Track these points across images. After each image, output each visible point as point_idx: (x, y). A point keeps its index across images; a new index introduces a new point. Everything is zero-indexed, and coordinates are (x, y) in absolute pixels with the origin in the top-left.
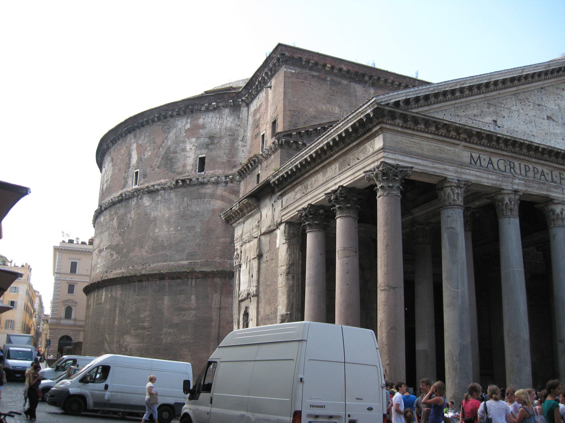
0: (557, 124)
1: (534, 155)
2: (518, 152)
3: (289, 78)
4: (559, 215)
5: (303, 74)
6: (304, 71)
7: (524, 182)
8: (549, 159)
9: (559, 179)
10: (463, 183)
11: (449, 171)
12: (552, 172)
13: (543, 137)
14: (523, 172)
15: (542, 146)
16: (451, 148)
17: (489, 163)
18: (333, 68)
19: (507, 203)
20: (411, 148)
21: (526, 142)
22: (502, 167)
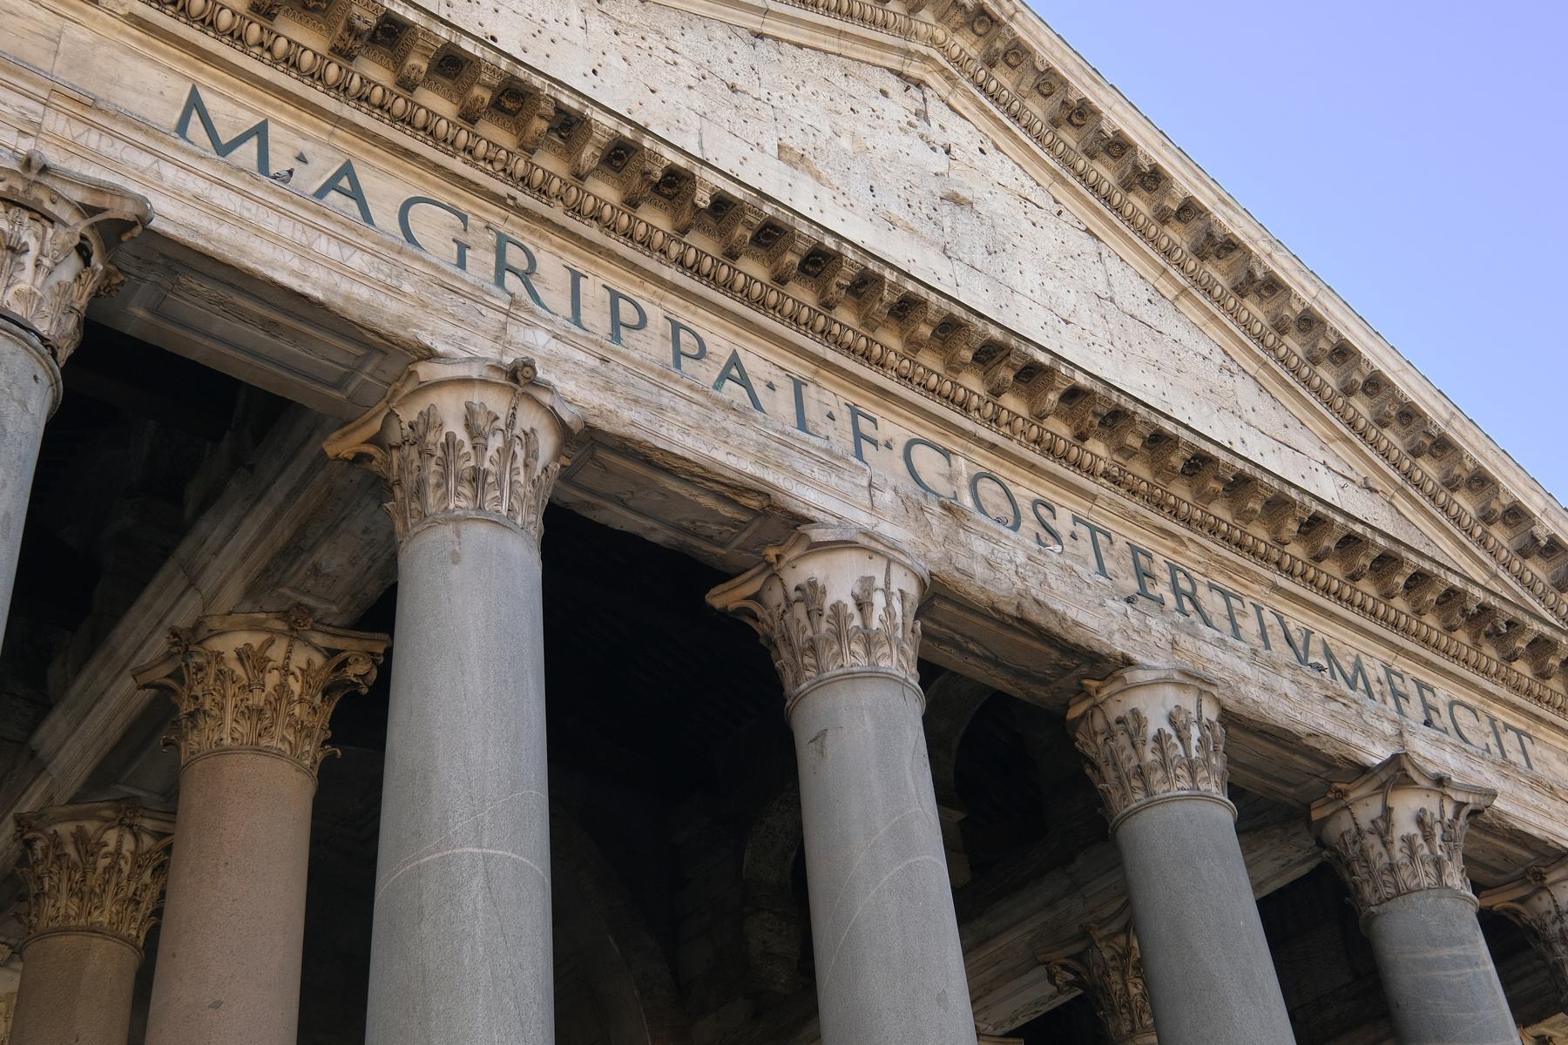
0: (843, 200)
2: (556, 183)
4: (852, 617)
8: (773, 298)
10: (78, 195)
12: (798, 385)
14: (596, 317)
17: (331, 185)
19: (450, 444)
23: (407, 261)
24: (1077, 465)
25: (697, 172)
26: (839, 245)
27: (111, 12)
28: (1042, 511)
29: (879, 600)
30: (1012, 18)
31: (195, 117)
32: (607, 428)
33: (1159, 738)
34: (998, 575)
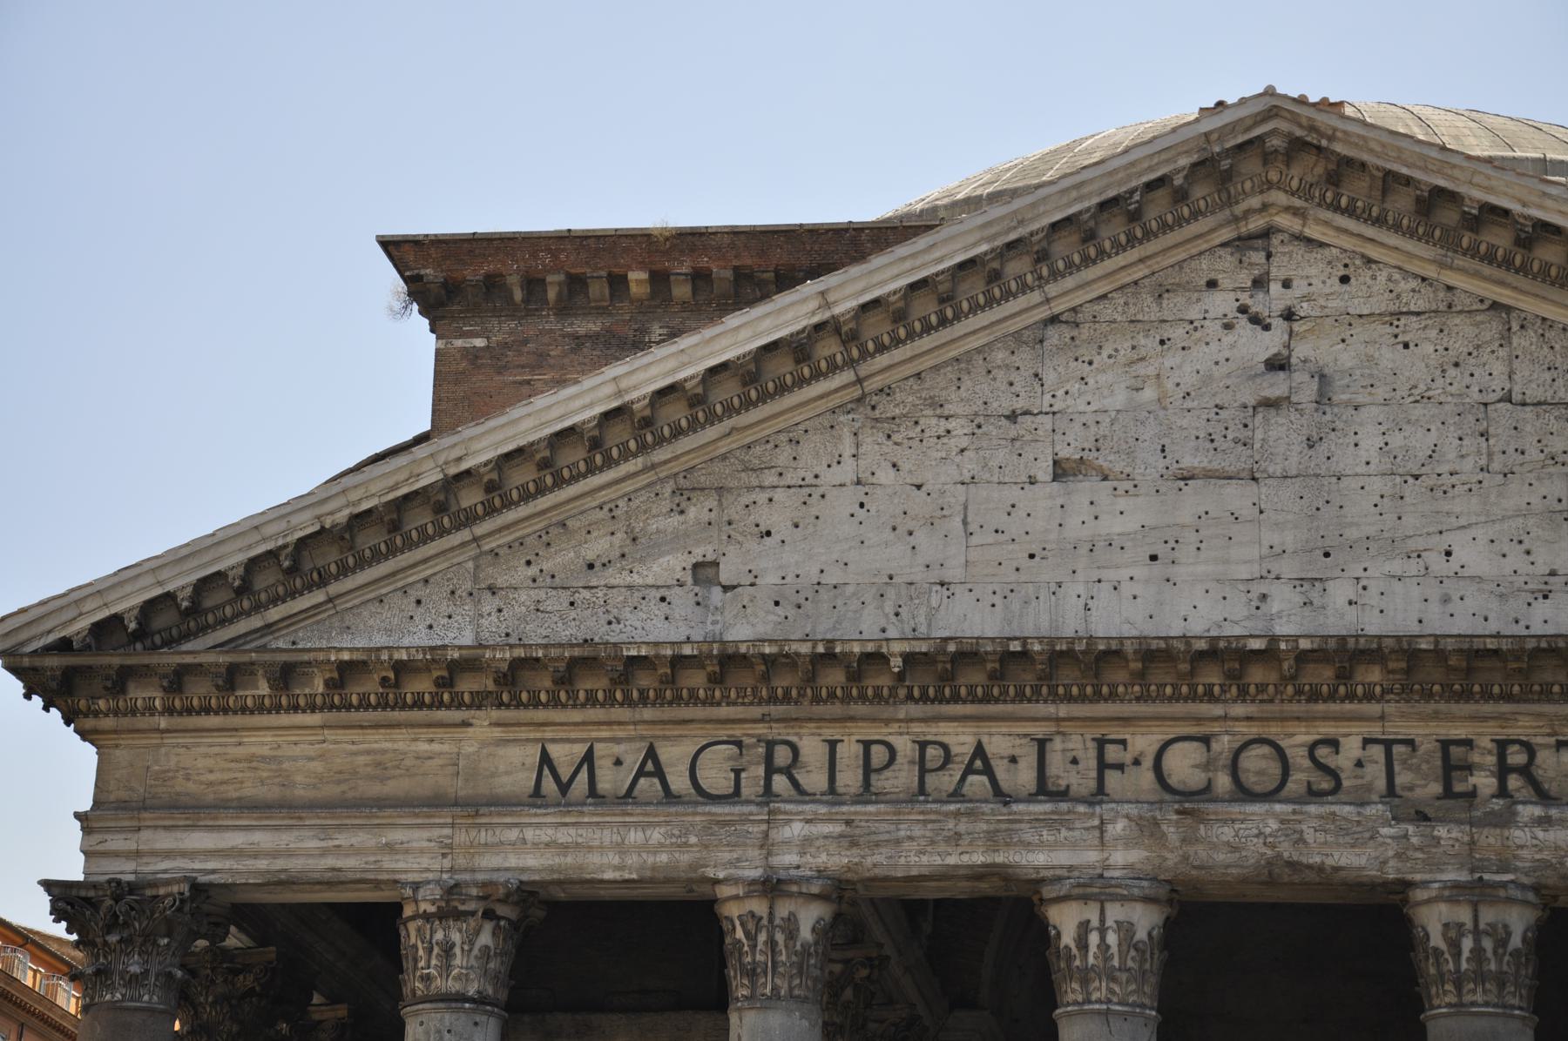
0: (1128, 485)
1: (892, 689)
2: (794, 693)
3: (457, 382)
5: (525, 342)
6: (531, 328)
7: (838, 828)
9: (1094, 774)
10: (474, 892)
11: (407, 851)
12: (1042, 744)
13: (1013, 577)
14: (849, 779)
15: (897, 647)
16: (436, 747)
17: (641, 773)
18: (660, 279)
20: (231, 787)
21: (795, 647)
22: (715, 776)
23: (690, 818)
24: (1351, 697)
25: (884, 650)
26: (1024, 644)
27: (481, 726)
28: (1323, 752)
29: (1094, 938)
30: (1331, 138)
31: (546, 771)
32: (856, 878)
33: (1437, 952)
34: (1244, 854)
